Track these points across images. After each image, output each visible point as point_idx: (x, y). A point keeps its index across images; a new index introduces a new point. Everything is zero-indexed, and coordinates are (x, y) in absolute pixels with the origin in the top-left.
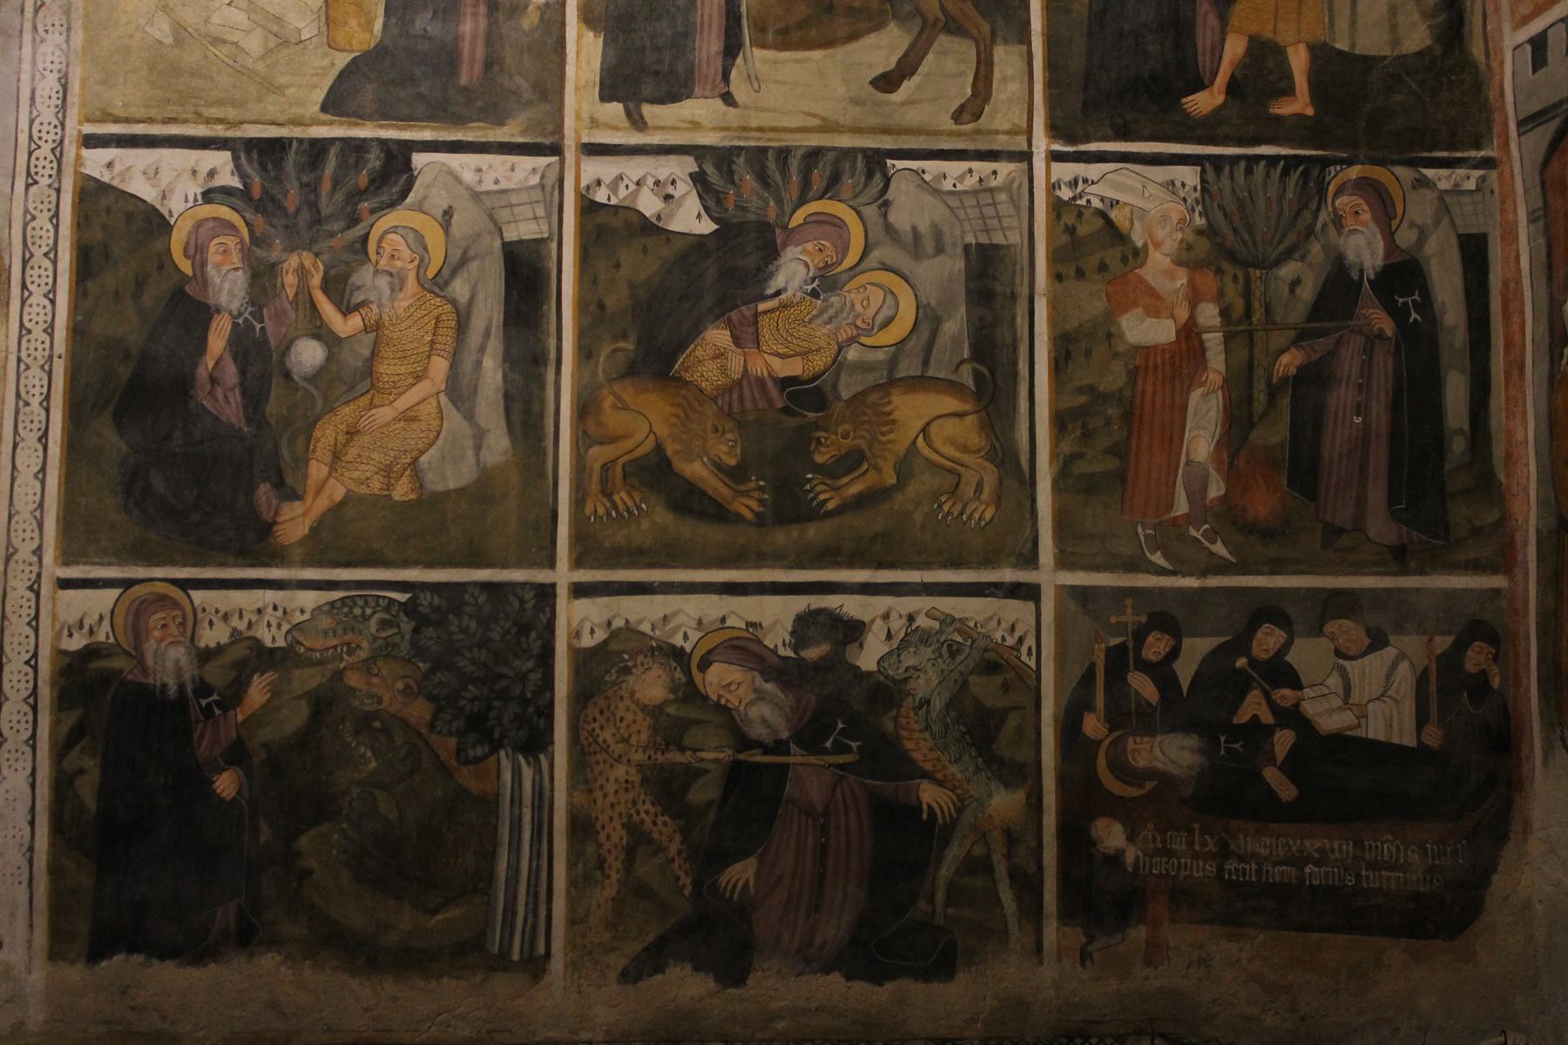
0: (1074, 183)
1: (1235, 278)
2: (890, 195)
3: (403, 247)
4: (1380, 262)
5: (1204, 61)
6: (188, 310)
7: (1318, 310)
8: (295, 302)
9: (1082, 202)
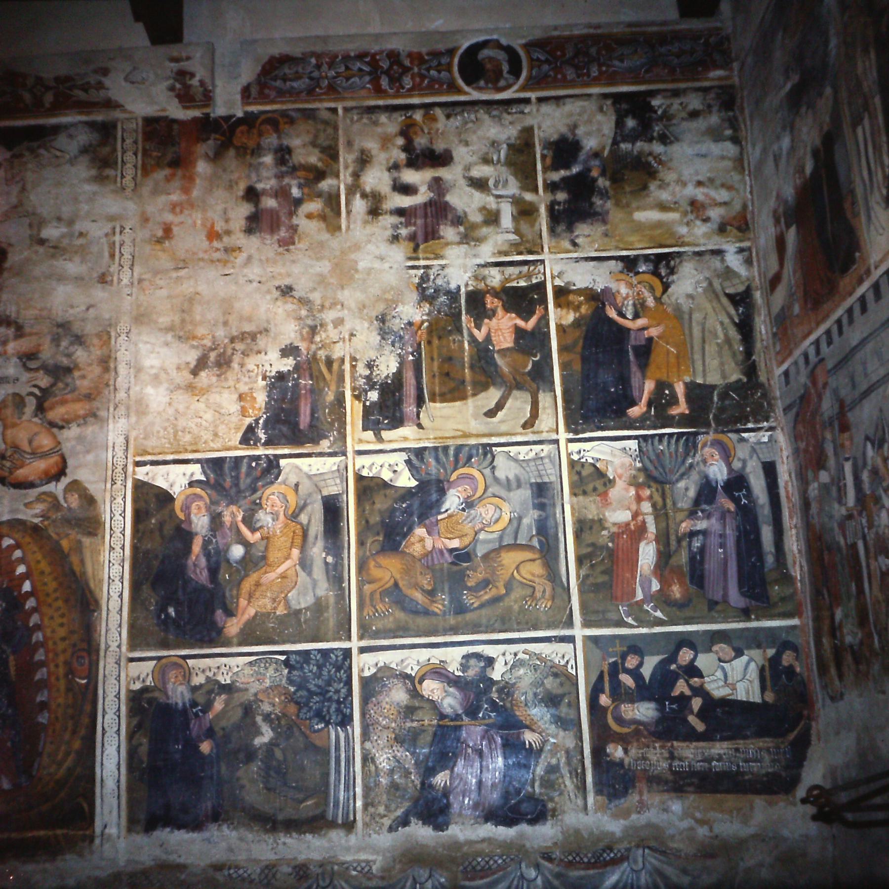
0: (579, 452)
1: (657, 490)
2: (495, 463)
3: (278, 502)
4: (725, 477)
5: (636, 393)
6: (183, 535)
7: (697, 502)
8: (230, 529)
9: (583, 460)
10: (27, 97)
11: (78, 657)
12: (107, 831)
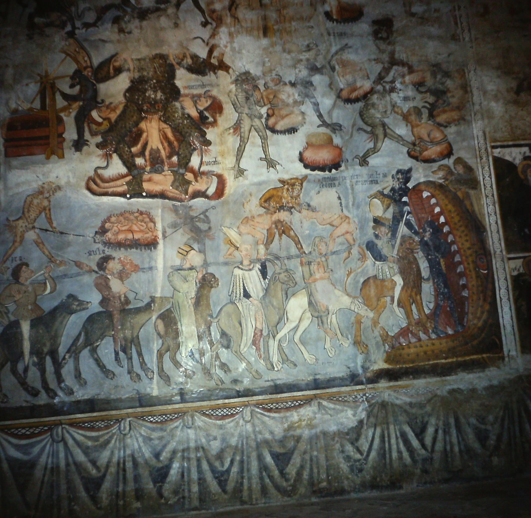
11: (480, 259)
12: (511, 353)
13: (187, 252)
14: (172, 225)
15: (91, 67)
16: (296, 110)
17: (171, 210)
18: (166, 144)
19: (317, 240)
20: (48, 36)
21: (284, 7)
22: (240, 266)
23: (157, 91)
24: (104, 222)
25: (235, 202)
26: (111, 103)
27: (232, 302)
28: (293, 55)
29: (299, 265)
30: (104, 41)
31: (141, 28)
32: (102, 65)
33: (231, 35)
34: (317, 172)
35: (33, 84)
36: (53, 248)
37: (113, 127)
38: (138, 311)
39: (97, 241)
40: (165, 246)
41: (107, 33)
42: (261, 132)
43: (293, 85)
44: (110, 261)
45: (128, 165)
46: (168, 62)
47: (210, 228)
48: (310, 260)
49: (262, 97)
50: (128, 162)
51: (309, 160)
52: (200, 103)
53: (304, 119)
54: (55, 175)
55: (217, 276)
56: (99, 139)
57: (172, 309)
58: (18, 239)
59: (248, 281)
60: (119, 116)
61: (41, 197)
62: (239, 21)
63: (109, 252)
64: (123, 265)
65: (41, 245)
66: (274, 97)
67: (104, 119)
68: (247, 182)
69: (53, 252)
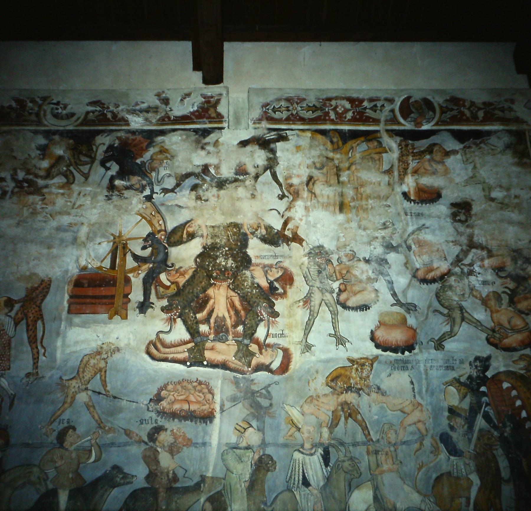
10: (467, 113)
13: (245, 429)
14: (231, 398)
15: (165, 231)
16: (369, 287)
17: (232, 383)
18: (232, 313)
19: (386, 427)
20: (127, 198)
21: (362, 186)
22: (301, 450)
23: (228, 258)
24: (161, 389)
25: (300, 379)
26: (181, 267)
27: (289, 490)
28: (369, 232)
29: (365, 453)
30: (180, 207)
31: (218, 196)
32: (175, 230)
33: (306, 208)
34: (388, 353)
35: (106, 243)
36: (103, 413)
37: (179, 292)
38: (187, 490)
39: (151, 409)
40: (221, 421)
41: (185, 199)
42: (332, 307)
43: (367, 261)
44: (161, 433)
45: (192, 331)
46: (242, 231)
47: (271, 405)
48: (378, 449)
49: (335, 272)
50: (192, 328)
51: (381, 339)
52: (271, 273)
53: (377, 296)
54: (116, 336)
55: (275, 458)
56: (165, 302)
57: (223, 492)
58: (69, 400)
59: (309, 467)
60: (188, 281)
61: (98, 357)
62: (315, 196)
63: (161, 422)
64: (175, 438)
65: (92, 409)
66: (347, 272)
67: (172, 283)
68: (313, 358)
69: (103, 417)
